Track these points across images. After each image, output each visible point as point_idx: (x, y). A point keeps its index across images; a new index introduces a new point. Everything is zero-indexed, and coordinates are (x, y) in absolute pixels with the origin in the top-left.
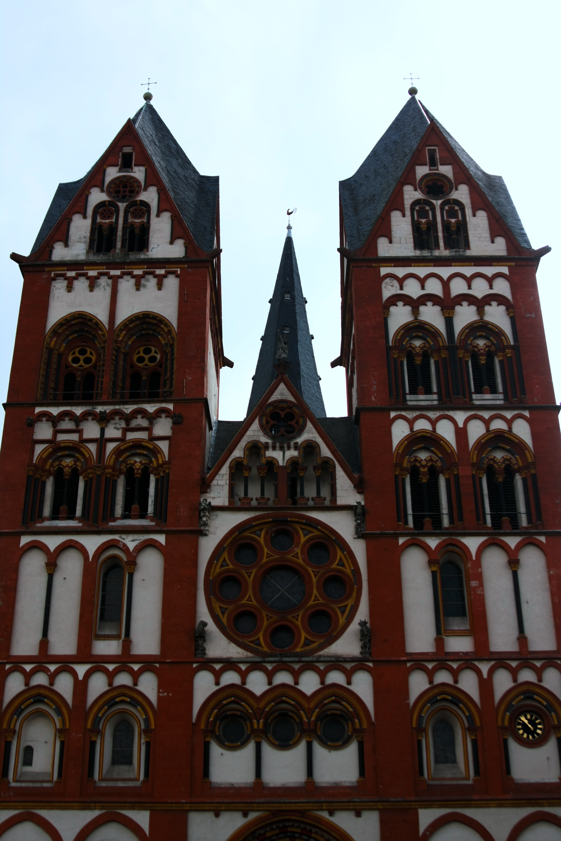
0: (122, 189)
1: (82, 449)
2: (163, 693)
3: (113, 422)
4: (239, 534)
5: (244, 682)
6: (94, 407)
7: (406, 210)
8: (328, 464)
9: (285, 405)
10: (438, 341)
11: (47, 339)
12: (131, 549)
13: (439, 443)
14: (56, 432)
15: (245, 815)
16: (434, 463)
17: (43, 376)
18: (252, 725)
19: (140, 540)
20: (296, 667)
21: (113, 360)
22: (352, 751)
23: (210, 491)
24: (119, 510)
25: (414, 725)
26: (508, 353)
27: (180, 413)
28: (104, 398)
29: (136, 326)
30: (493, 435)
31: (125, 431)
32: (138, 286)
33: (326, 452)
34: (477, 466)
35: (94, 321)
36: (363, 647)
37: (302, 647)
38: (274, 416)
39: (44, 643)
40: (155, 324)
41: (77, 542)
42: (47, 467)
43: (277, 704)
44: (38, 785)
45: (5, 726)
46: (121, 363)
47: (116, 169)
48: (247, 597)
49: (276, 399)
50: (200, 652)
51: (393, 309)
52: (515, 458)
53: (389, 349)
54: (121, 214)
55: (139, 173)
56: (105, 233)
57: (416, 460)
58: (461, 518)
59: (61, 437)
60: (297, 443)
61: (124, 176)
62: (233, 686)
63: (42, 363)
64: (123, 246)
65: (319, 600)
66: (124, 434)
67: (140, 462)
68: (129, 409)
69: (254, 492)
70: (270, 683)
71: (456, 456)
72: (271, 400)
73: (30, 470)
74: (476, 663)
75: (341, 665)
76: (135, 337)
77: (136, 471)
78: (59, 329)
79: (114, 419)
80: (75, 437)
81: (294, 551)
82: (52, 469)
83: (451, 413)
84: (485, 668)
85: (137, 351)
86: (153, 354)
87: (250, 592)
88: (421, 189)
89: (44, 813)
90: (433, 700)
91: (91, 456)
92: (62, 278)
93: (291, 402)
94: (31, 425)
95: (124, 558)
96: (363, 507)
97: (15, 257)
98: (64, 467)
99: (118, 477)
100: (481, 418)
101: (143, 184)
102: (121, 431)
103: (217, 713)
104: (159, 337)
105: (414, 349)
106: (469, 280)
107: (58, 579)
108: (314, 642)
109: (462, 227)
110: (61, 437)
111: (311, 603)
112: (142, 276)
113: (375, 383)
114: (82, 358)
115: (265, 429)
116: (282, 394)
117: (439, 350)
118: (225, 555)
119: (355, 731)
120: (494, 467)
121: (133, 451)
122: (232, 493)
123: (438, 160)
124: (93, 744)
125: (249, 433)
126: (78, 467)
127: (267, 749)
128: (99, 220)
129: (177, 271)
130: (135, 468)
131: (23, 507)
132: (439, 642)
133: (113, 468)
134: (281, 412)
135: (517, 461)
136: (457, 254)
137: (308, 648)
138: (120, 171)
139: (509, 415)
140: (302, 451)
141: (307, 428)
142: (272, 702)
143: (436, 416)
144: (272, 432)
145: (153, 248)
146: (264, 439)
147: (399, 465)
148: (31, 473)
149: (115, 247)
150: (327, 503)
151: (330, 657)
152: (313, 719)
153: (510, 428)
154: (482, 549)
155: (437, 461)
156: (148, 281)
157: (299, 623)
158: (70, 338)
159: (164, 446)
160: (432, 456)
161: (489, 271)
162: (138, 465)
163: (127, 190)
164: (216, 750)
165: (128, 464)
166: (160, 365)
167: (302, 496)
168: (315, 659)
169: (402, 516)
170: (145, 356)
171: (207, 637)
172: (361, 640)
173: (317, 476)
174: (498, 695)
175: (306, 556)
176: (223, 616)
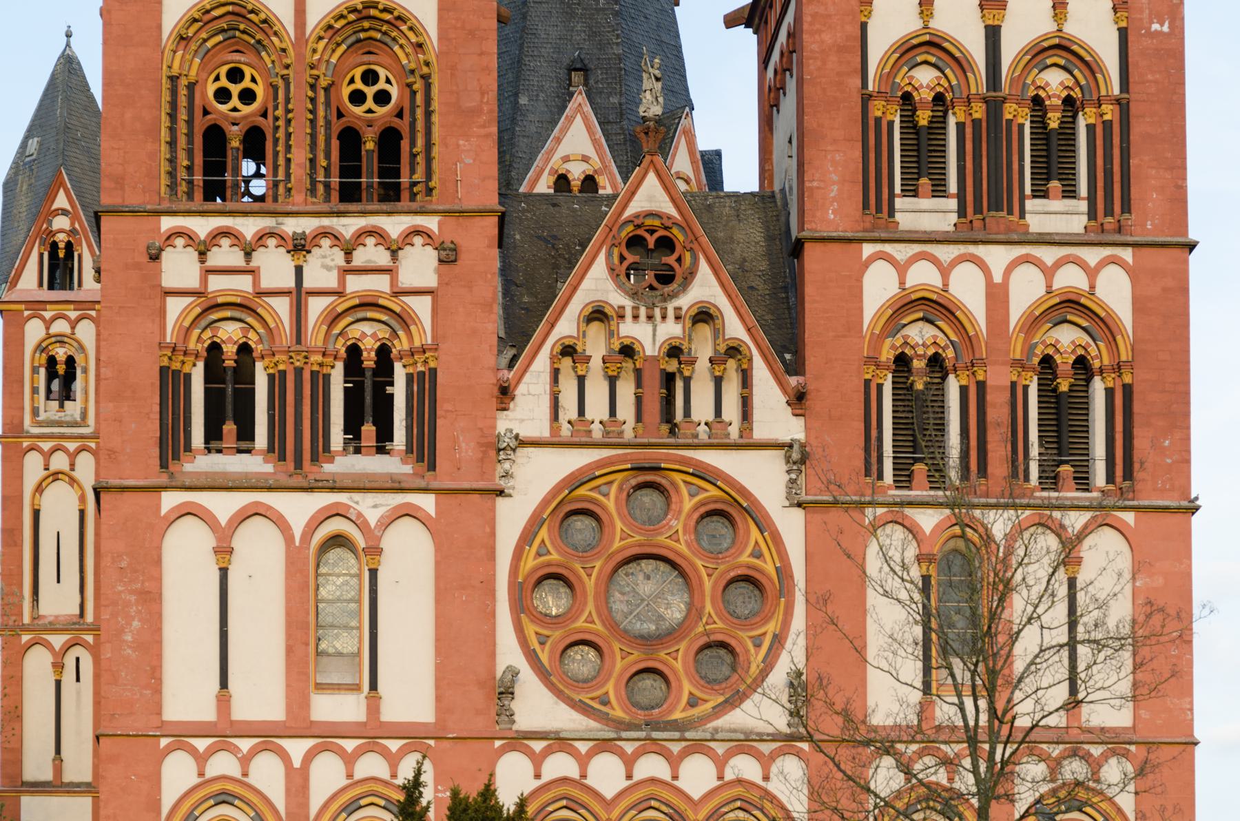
1: (260, 310)
2: (444, 791)
3: (315, 251)
4: (570, 493)
5: (584, 776)
9: (657, 223)
12: (373, 524)
16: (940, 351)
19: (388, 505)
20: (676, 748)
23: (515, 406)
27: (452, 242)
28: (299, 199)
29: (349, 23)
30: (1057, 300)
33: (735, 328)
35: (263, 16)
37: (683, 710)
38: (635, 242)
40: (388, 22)
41: (270, 508)
42: (192, 345)
43: (640, 812)
46: (321, 112)
48: (586, 614)
49: (639, 210)
50: (506, 719)
57: (906, 343)
58: (983, 470)
59: (216, 283)
60: (680, 309)
62: (565, 780)
63: (163, 114)
65: (715, 623)
66: (342, 282)
67: (374, 335)
68: (348, 226)
69: (597, 407)
70: (629, 777)
72: (629, 212)
75: (753, 746)
76: (344, 47)
77: (365, 354)
81: (671, 527)
83: (980, 251)
86: (381, 85)
87: (591, 607)
91: (280, 325)
93: (669, 217)
96: (803, 446)
102: (335, 273)
104: (396, 48)
108: (706, 701)
110: (216, 283)
113: (835, 178)
116: (651, 198)
118: (544, 533)
120: (1055, 361)
121: (360, 315)
125: (586, 284)
126: (250, 342)
130: (363, 347)
131: (158, 435)
134: (647, 236)
135: (1099, 355)
137: (696, 712)
139: (1092, 256)
140: (688, 323)
141: (699, 276)
142: (631, 808)
144: (629, 279)
146: (616, 298)
147: (873, 361)
148: (165, 362)
151: (735, 731)
153: (1092, 287)
157: (679, 665)
158: (209, 44)
159: (421, 307)
160: (937, 337)
167: (688, 420)
168: (708, 736)
169: (872, 467)
176: (543, 651)
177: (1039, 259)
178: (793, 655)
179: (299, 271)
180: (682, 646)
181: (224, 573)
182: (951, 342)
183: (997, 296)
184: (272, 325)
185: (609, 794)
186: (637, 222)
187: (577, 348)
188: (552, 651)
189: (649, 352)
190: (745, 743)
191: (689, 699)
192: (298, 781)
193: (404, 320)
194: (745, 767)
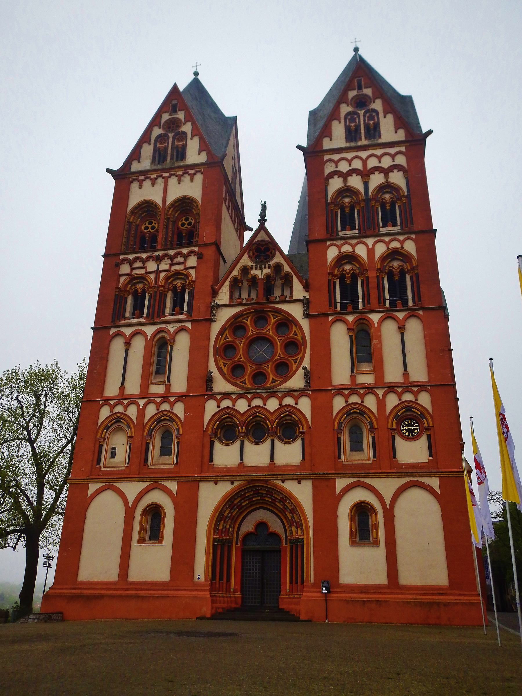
0: (171, 126)
1: (146, 277)
3: (164, 260)
5: (234, 406)
6: (153, 253)
7: (341, 119)
8: (289, 275)
9: (264, 243)
10: (359, 197)
11: (128, 217)
13: (356, 258)
14: (132, 269)
15: (232, 483)
16: (355, 271)
17: (125, 238)
18: (239, 431)
20: (265, 395)
21: (165, 225)
22: (298, 443)
24: (168, 311)
25: (336, 428)
26: (404, 200)
28: (159, 247)
29: (179, 204)
31: (171, 265)
32: (179, 181)
33: (287, 269)
34: (379, 270)
35: (154, 204)
36: (306, 382)
38: (258, 250)
39: (122, 388)
42: (128, 289)
44: (117, 469)
45: (99, 436)
47: (168, 114)
51: (331, 181)
52: (406, 264)
53: (327, 204)
54: (171, 140)
55: (181, 115)
56: (162, 152)
57: (343, 270)
58: (369, 303)
59: (135, 272)
60: (270, 264)
61: (172, 118)
63: (125, 231)
64: (172, 158)
66: (170, 267)
68: (172, 252)
70: (249, 406)
71: (367, 266)
72: (255, 241)
73: (117, 291)
74: (375, 390)
76: (179, 212)
77: (178, 288)
78: (135, 210)
79: (165, 259)
80: (143, 271)
82: (131, 291)
83: (365, 240)
84: (380, 393)
85: (181, 220)
86: (190, 221)
87: (241, 353)
88: (351, 104)
89: (118, 485)
90: (348, 414)
92: (137, 181)
93: (267, 241)
94: (118, 266)
95: (168, 337)
97: (108, 171)
98: (138, 289)
99: (168, 292)
100: (383, 241)
101: (183, 121)
103: (219, 424)
104: (193, 210)
105: (345, 204)
106: (379, 158)
107: (131, 352)
108: (278, 381)
109: (377, 126)
110: (135, 272)
111: (276, 358)
112: (182, 175)
114: (150, 226)
115: (251, 258)
116: (262, 237)
117: (359, 202)
118: (227, 333)
119: (300, 432)
122: (231, 296)
123: (363, 86)
124: (148, 445)
125: (242, 261)
127: (247, 444)
128: (158, 145)
129: (202, 170)
132: (353, 377)
133: (164, 287)
135: (407, 266)
136: (373, 142)
138: (170, 115)
139: (401, 238)
140: (272, 269)
143: (355, 242)
144: (255, 259)
145: (188, 158)
146: (250, 264)
147: (331, 273)
148: (117, 293)
149: (167, 160)
150: (287, 299)
152: (274, 425)
153: (402, 246)
154: (382, 321)
155: (356, 270)
156: (185, 177)
157: (269, 370)
158: (143, 215)
159: (193, 272)
161: (392, 151)
162: (179, 285)
163: (175, 126)
164: (217, 445)
165: (174, 285)
166: (194, 226)
168: (276, 390)
170: (185, 222)
171: (214, 381)
172: (305, 378)
173: (282, 283)
174: (389, 409)
175: (274, 331)
177: (384, 240)
178: (306, 362)
179: (158, 266)
180: (270, 364)
181: (127, 351)
182: (357, 267)
183: (371, 252)
184: (150, 281)
185: (242, 411)
186: (257, 243)
187: (239, 279)
188: (228, 368)
189: (260, 277)
190: (289, 393)
191: (272, 380)
192: (141, 412)
193: (187, 276)
194: (289, 401)
